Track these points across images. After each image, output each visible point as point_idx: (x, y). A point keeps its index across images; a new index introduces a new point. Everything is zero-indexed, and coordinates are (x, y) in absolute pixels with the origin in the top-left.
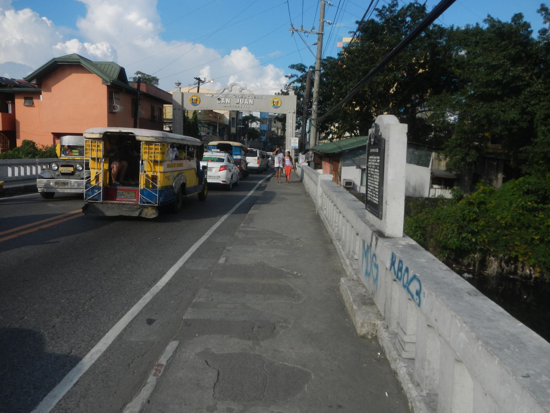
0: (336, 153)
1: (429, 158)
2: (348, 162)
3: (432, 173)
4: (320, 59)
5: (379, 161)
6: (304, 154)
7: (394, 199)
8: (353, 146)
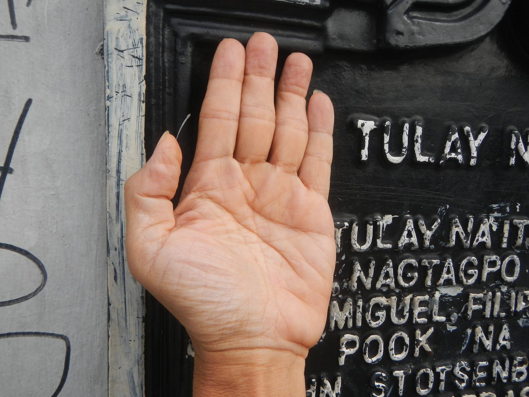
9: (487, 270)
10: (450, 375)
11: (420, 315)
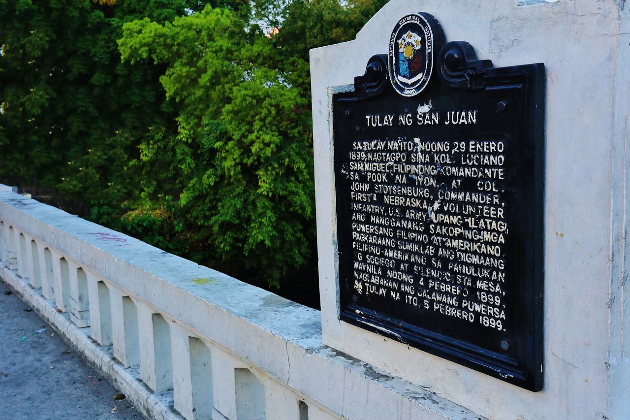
9: (397, 157)
10: (392, 188)
11: (383, 169)
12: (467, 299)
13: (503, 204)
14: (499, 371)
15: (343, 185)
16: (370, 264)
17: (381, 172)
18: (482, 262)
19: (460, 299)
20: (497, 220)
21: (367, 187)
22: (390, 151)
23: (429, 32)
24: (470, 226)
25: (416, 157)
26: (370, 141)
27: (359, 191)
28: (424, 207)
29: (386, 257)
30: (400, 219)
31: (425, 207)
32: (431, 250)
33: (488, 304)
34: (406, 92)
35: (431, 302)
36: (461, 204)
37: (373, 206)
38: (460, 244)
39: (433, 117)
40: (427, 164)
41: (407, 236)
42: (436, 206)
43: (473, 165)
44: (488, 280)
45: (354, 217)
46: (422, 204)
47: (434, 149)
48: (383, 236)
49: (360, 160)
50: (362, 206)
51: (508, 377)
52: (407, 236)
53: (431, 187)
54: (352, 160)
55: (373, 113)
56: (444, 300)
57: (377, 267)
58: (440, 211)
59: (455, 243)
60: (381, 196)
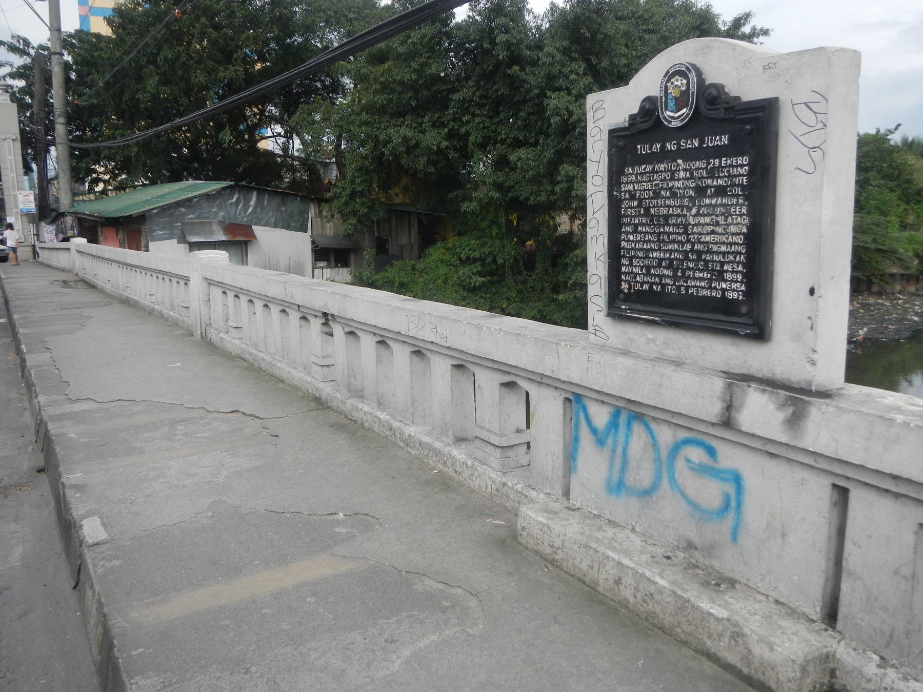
0: (134, 216)
1: (307, 216)
2: (161, 232)
3: (313, 242)
4: (59, 30)
5: (744, 171)
6: (52, 222)
7: (832, 278)
8: (165, 201)
9: (663, 176)
12: (716, 280)
13: (746, 203)
14: (738, 330)
15: (614, 204)
16: (636, 266)
17: (648, 190)
18: (729, 249)
19: (710, 281)
20: (741, 215)
21: (635, 203)
22: (657, 172)
23: (693, 77)
24: (720, 223)
25: (678, 174)
26: (640, 165)
27: (629, 208)
28: (684, 213)
29: (651, 258)
30: (664, 225)
31: (685, 212)
32: (688, 247)
33: (732, 281)
34: (673, 123)
35: (687, 288)
36: (715, 206)
37: (640, 218)
38: (712, 238)
39: (694, 142)
40: (687, 179)
41: (668, 238)
42: (694, 211)
43: (725, 176)
44: (733, 262)
45: (623, 230)
46: (682, 211)
47: (694, 166)
48: (649, 241)
49: (631, 182)
50: (631, 220)
51: (746, 333)
52: (668, 238)
53: (690, 197)
54: (623, 183)
55: (643, 143)
56: (698, 284)
57: (642, 268)
58: (698, 214)
59: (708, 238)
60: (647, 210)
